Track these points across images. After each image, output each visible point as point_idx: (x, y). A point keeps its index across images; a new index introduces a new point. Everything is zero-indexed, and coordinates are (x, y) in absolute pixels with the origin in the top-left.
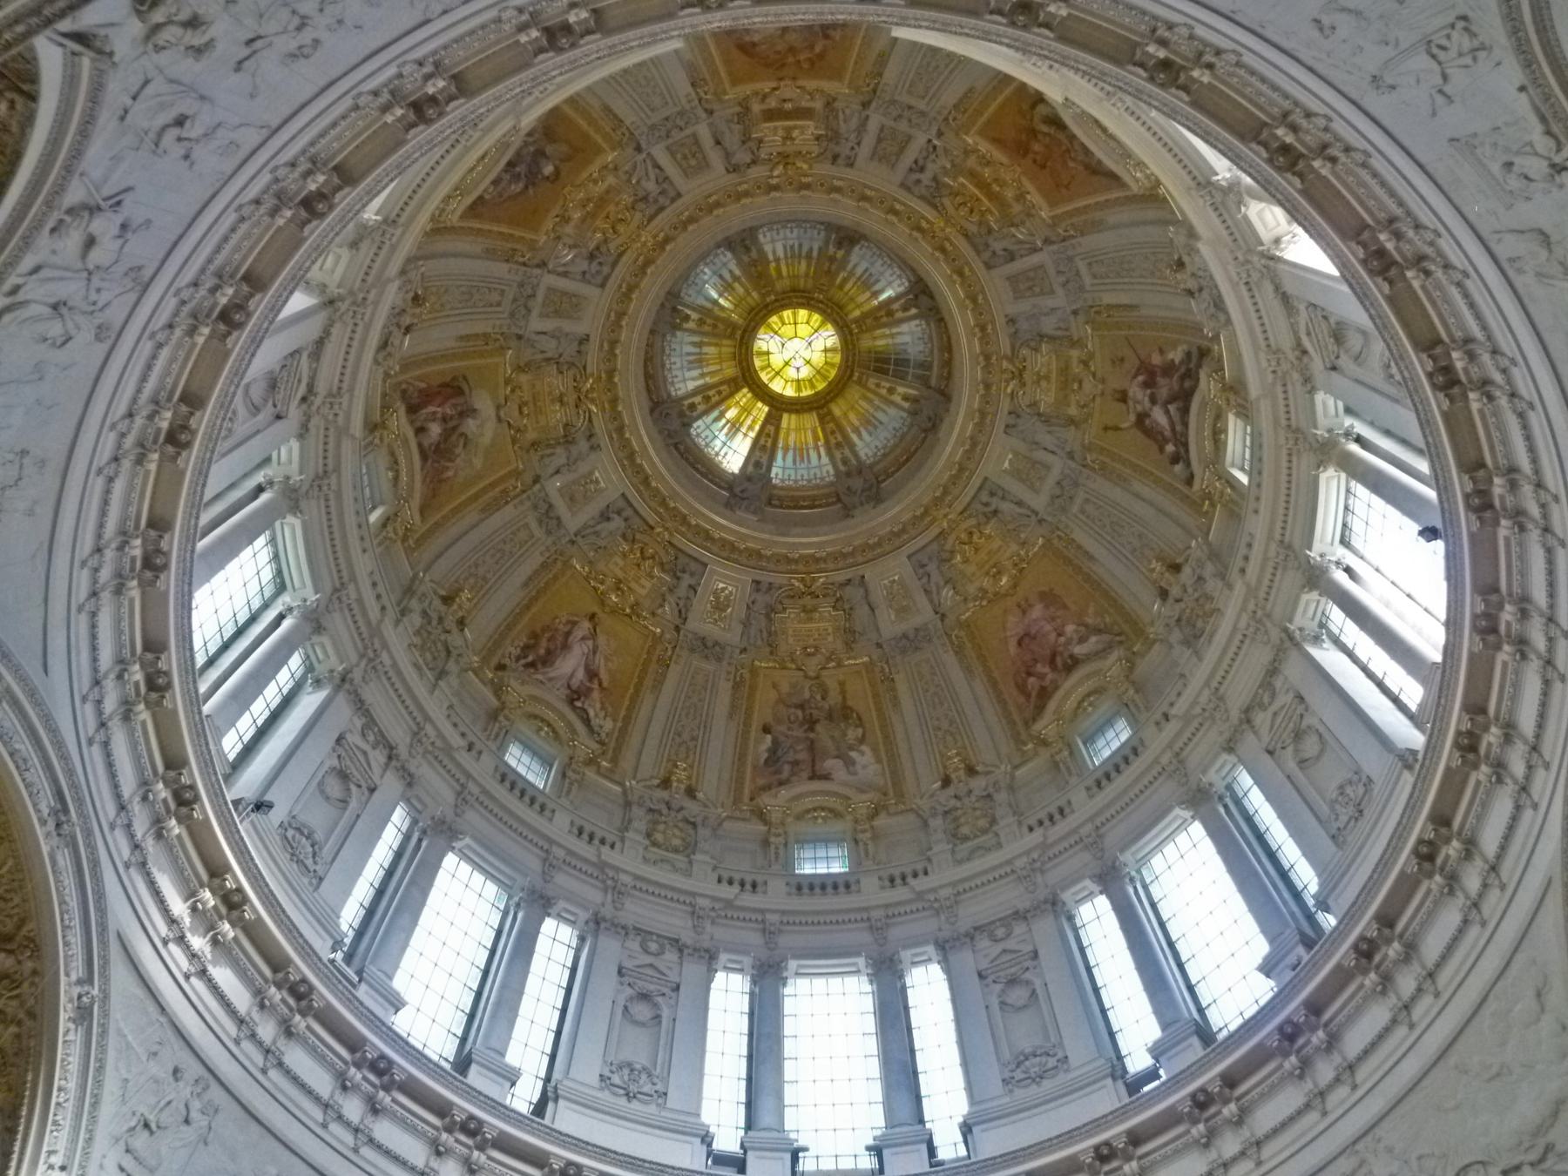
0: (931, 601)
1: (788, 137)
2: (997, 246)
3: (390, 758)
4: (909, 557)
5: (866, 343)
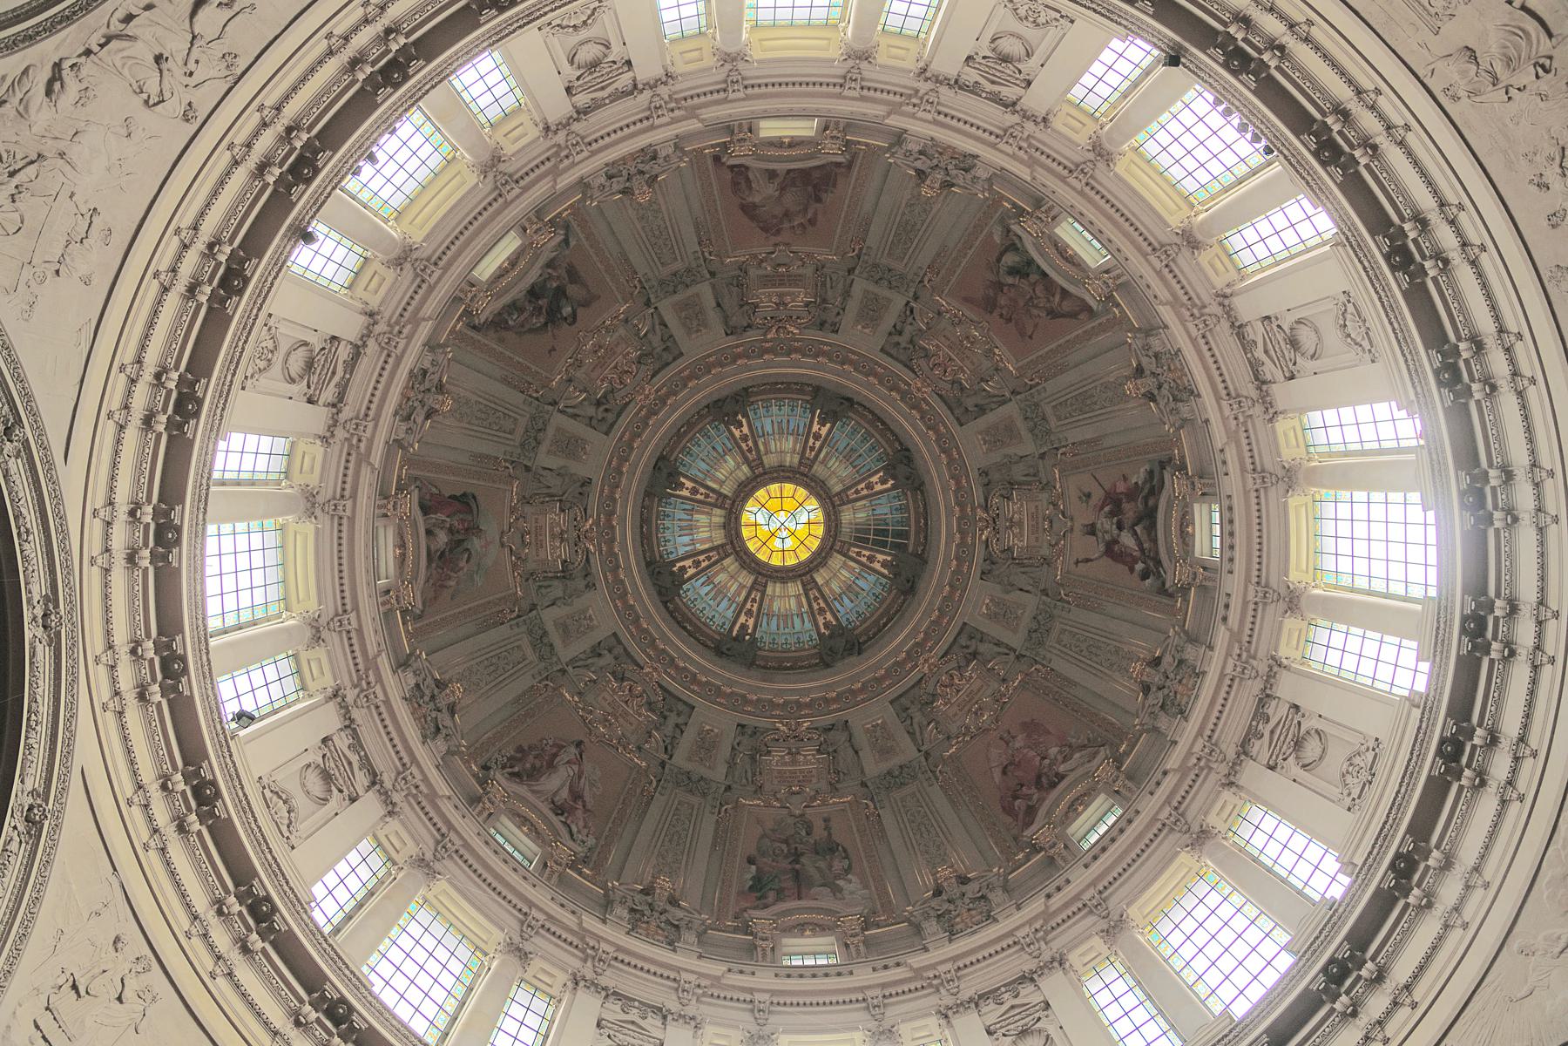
0: (914, 740)
2: (970, 403)
3: (373, 783)
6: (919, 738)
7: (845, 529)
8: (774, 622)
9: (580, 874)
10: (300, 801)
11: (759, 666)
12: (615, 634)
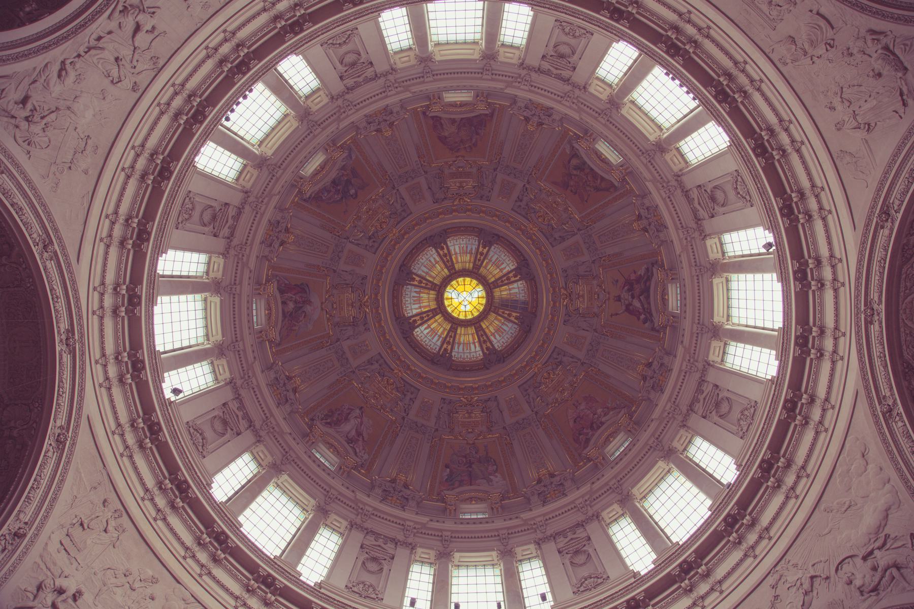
0: (530, 406)
1: (461, 187)
4: (519, 387)
5: (497, 293)
6: (532, 403)
7: (496, 300)
8: (461, 347)
9: (359, 472)
10: (209, 434)
11: (454, 370)
12: (379, 353)
